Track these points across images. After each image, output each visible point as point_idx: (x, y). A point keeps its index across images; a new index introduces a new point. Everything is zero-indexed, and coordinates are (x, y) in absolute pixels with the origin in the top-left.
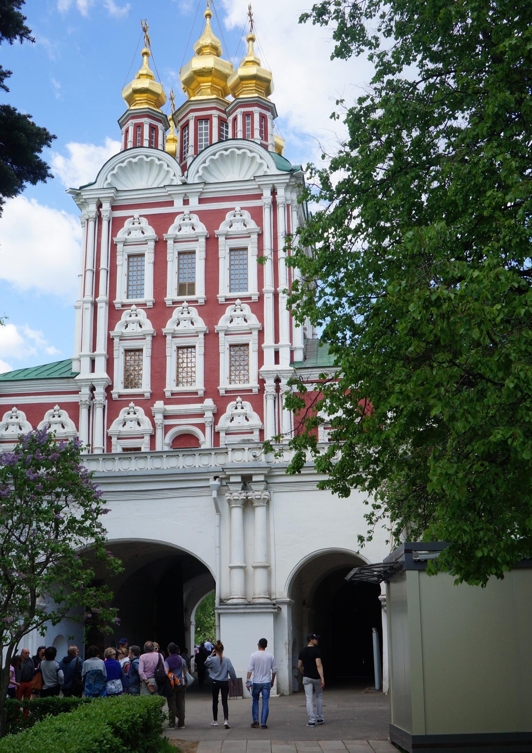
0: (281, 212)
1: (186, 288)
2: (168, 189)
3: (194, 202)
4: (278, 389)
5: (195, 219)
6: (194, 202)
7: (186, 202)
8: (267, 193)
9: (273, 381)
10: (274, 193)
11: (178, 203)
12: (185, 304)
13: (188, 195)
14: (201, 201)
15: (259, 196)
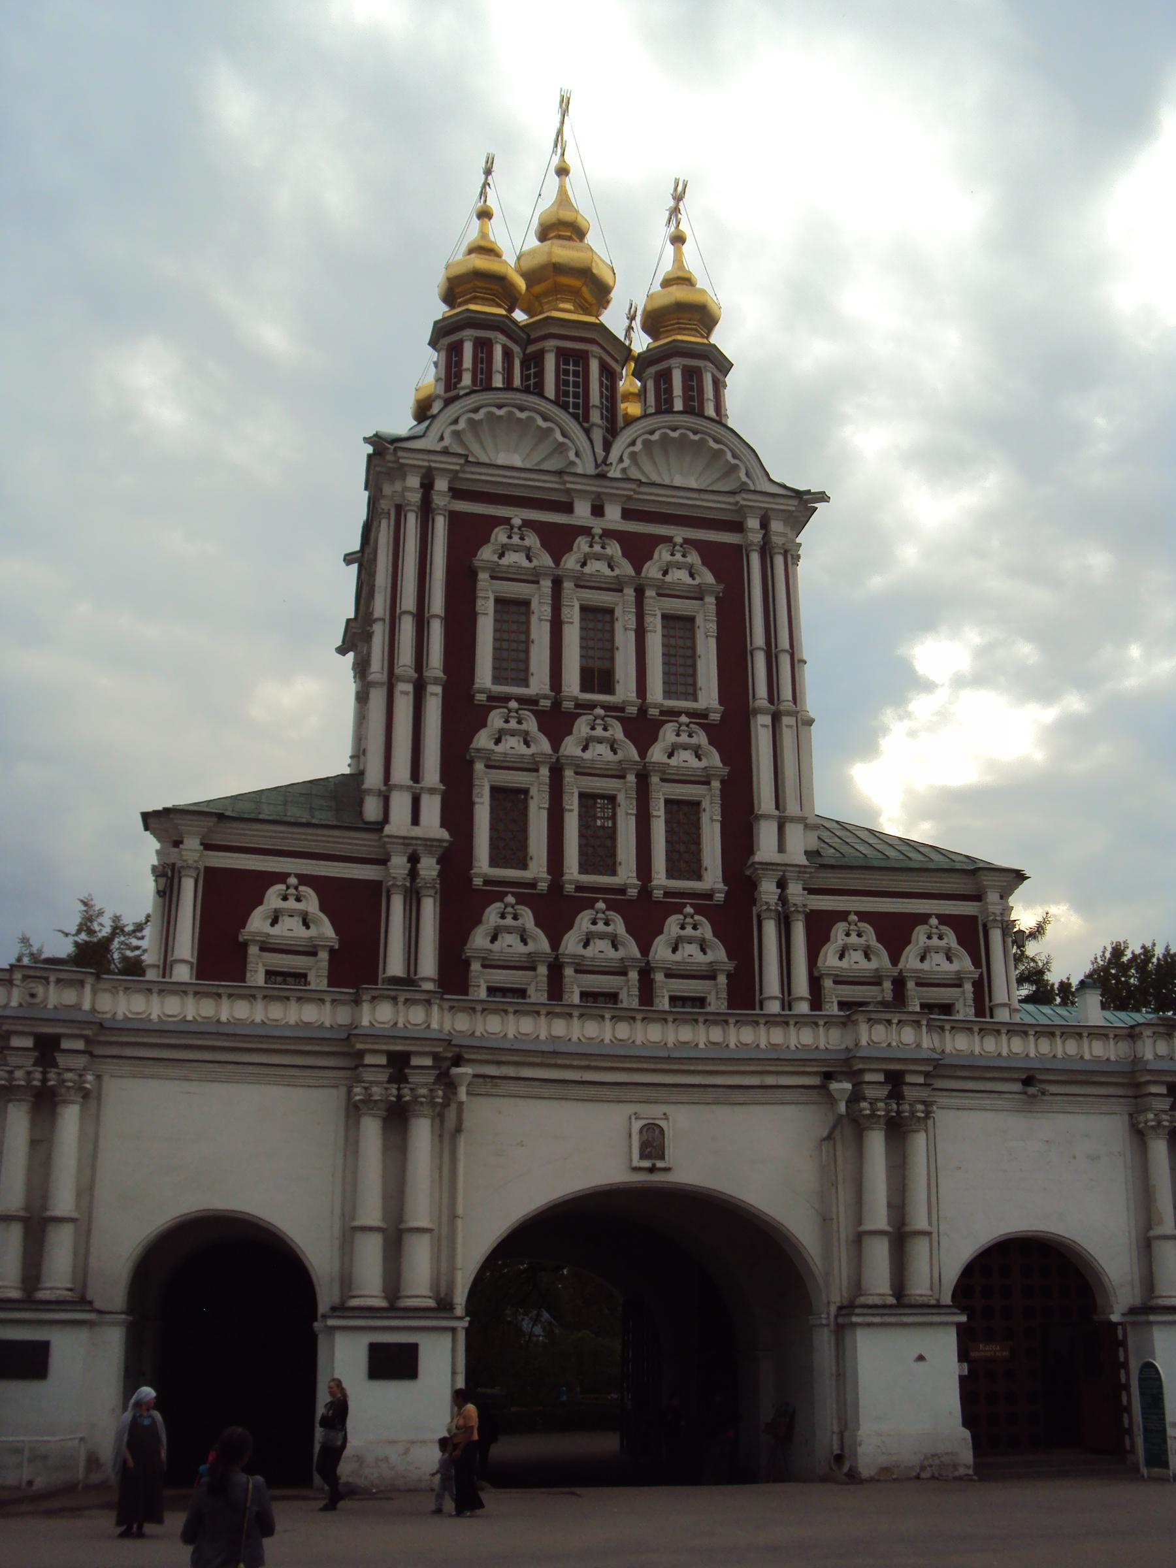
0: (779, 561)
1: (599, 677)
2: (567, 478)
3: (613, 513)
4: (783, 899)
5: (614, 549)
6: (613, 513)
7: (598, 511)
8: (753, 523)
9: (775, 884)
10: (765, 525)
11: (582, 512)
12: (599, 711)
13: (604, 497)
14: (627, 514)
15: (738, 527)
